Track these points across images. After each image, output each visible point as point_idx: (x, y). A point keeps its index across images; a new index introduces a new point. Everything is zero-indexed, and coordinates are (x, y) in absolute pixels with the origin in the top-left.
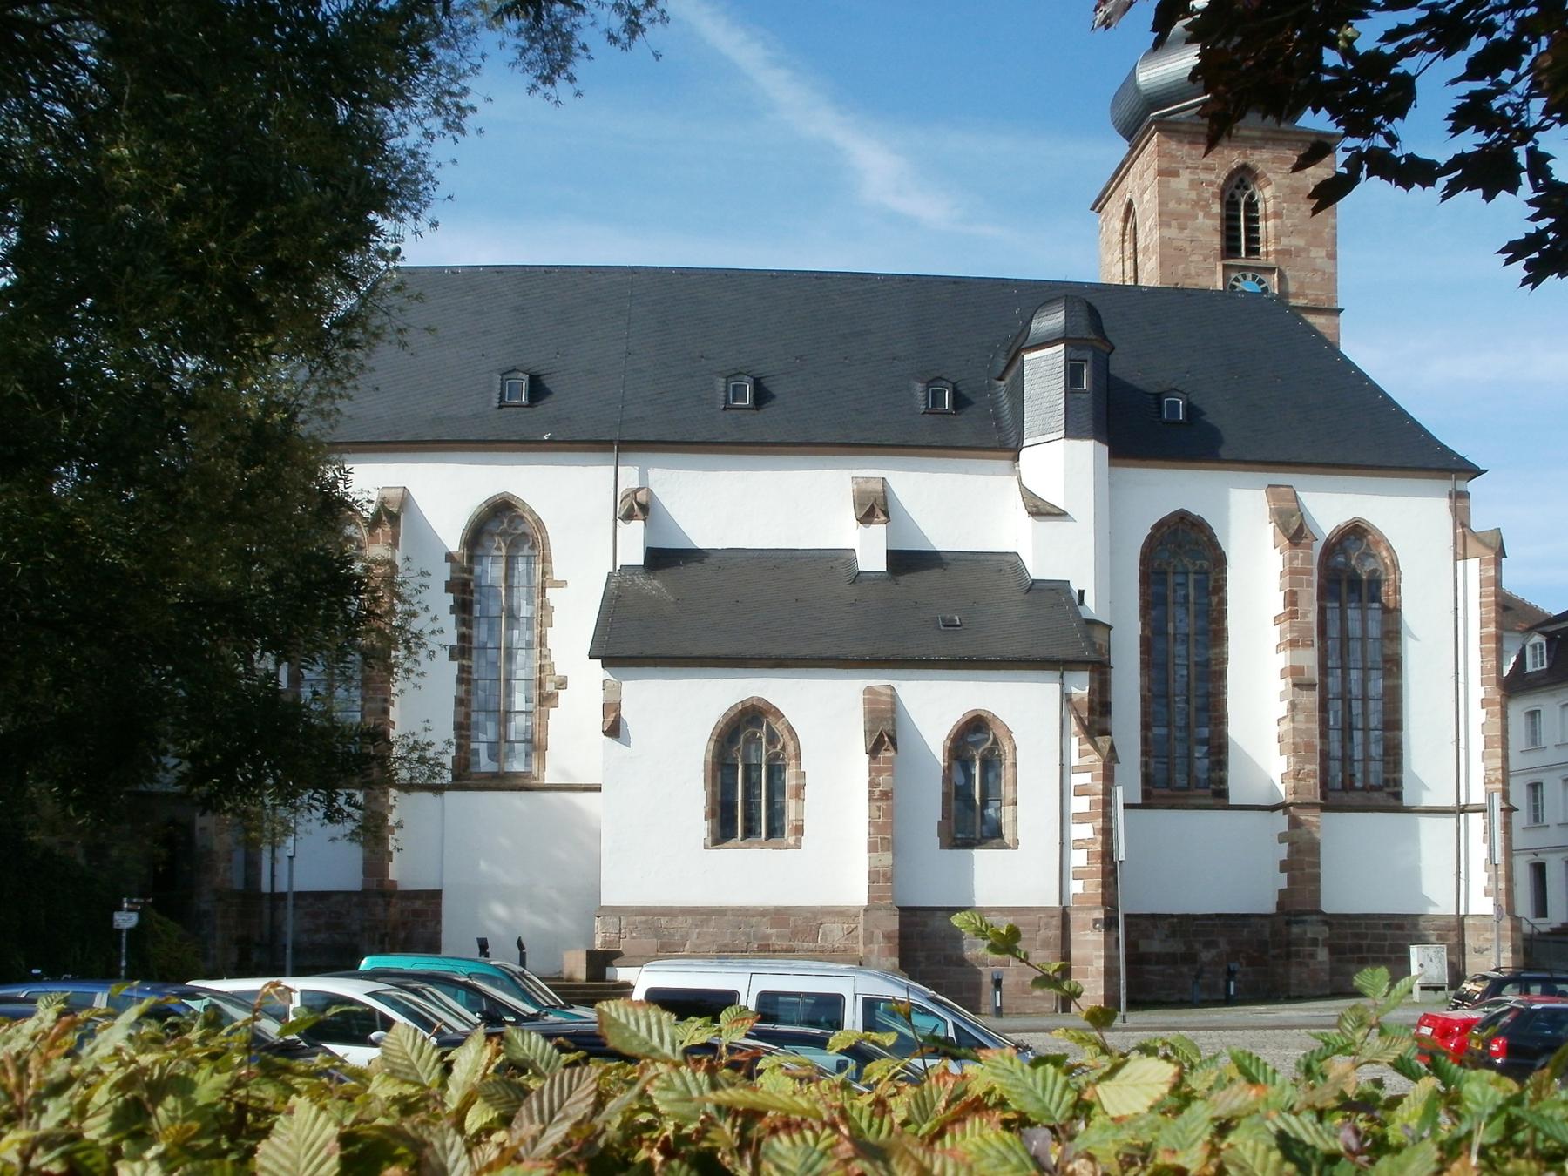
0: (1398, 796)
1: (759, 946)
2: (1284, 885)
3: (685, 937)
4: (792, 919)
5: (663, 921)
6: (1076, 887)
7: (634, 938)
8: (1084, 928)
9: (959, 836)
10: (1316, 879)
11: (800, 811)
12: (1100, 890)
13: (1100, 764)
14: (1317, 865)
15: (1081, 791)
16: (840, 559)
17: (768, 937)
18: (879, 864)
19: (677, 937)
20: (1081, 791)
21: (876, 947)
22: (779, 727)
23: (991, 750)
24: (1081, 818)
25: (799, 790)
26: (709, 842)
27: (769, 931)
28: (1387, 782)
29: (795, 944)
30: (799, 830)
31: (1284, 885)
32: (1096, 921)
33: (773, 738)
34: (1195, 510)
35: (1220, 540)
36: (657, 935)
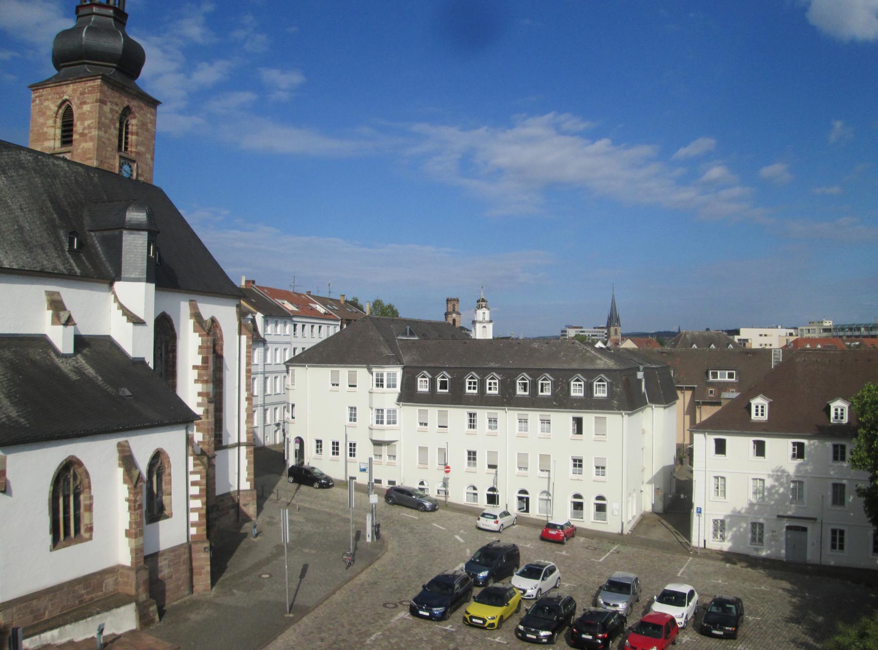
1: (80, 601)
5: (35, 602)
6: (193, 531)
7: (20, 618)
8: (199, 551)
11: (91, 518)
12: (205, 532)
13: (204, 471)
15: (194, 484)
16: (42, 341)
19: (42, 610)
20: (194, 484)
22: (80, 470)
23: (159, 467)
24: (195, 497)
30: (90, 529)
33: (75, 477)
35: (175, 327)
36: (32, 612)
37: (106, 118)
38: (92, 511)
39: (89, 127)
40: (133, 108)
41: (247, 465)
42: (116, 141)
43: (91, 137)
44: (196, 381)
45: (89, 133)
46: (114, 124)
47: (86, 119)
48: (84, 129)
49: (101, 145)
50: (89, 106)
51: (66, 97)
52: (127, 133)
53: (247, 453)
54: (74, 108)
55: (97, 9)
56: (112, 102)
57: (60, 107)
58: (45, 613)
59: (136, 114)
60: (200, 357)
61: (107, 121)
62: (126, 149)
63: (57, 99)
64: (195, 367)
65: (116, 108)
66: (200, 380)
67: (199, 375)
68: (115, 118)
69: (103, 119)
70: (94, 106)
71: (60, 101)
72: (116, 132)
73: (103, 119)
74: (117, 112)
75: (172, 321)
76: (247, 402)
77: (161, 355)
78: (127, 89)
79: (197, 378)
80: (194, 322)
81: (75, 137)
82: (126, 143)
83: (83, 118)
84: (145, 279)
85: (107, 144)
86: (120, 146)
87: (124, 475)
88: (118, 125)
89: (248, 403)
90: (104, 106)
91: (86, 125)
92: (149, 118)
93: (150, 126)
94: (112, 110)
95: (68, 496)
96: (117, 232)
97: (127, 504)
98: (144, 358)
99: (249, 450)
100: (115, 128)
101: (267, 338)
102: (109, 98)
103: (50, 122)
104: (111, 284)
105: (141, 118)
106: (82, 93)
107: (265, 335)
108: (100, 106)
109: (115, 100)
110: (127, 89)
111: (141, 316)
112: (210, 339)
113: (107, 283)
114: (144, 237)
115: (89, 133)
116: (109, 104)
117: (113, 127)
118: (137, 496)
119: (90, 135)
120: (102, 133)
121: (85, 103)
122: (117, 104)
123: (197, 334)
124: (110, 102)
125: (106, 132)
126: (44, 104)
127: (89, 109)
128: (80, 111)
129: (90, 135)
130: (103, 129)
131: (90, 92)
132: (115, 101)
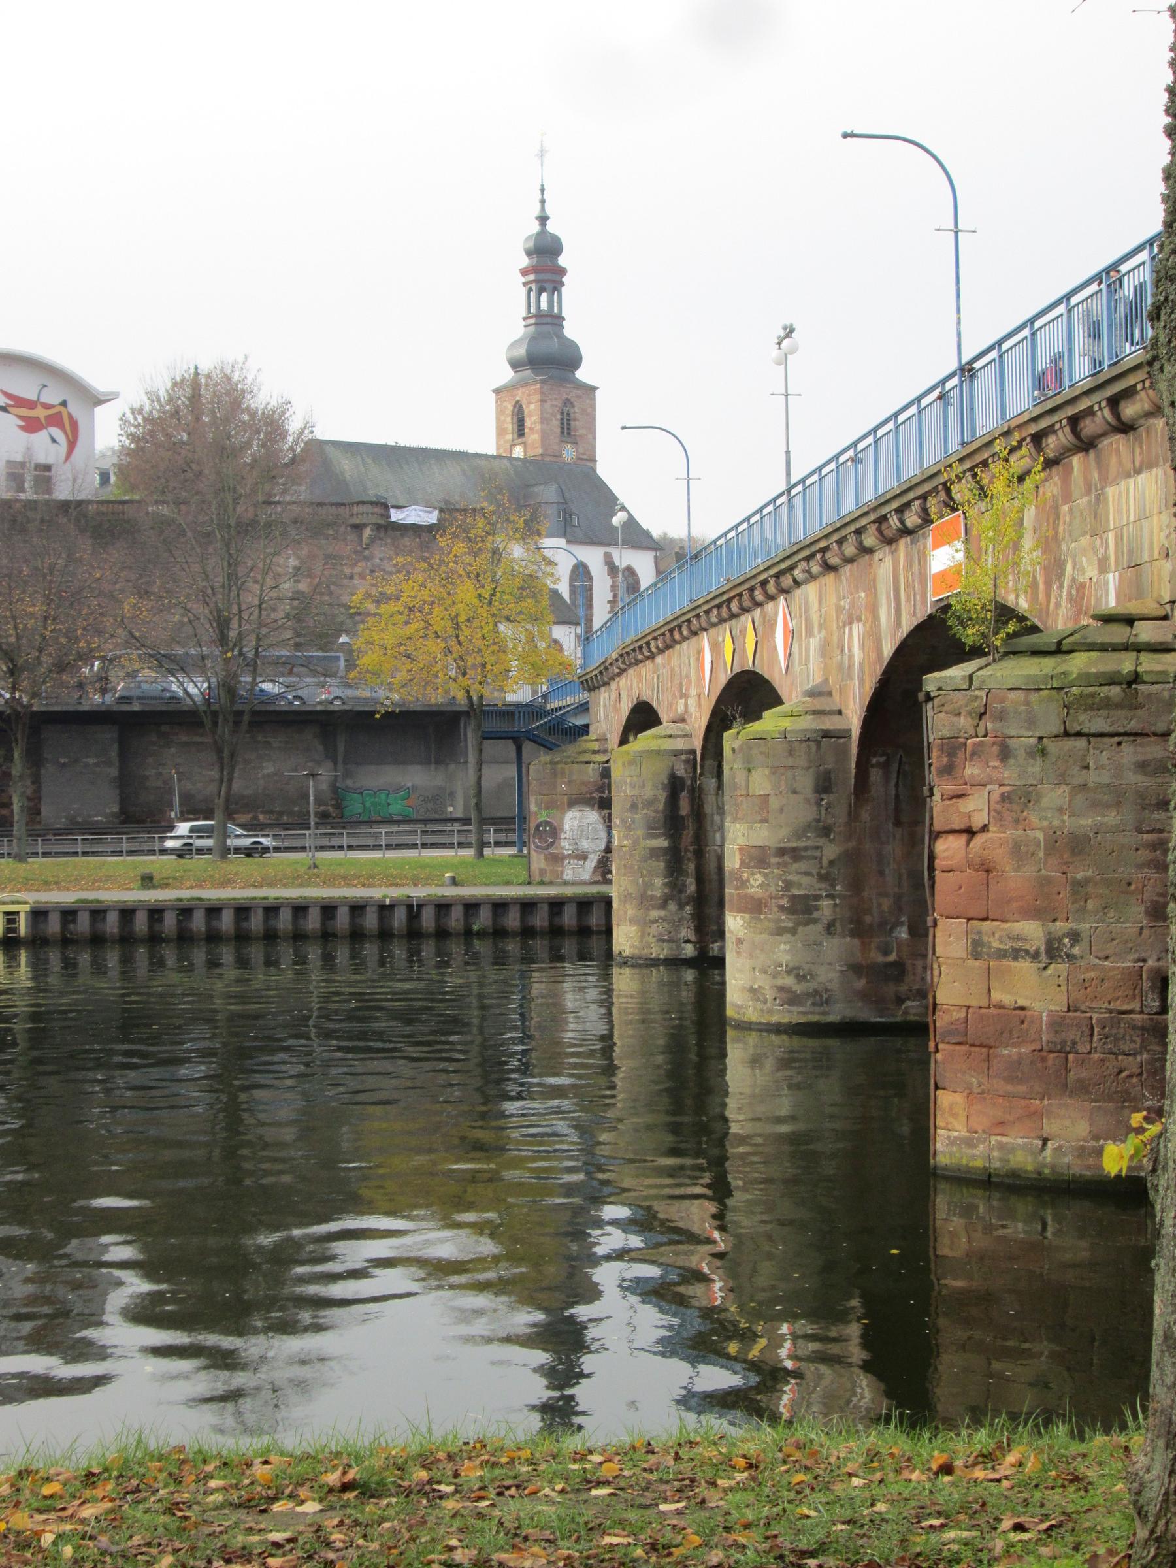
39: (535, 423)
42: (558, 430)
49: (544, 436)
57: (515, 406)
62: (569, 433)
64: (609, 602)
65: (555, 403)
67: (612, 608)
72: (558, 423)
81: (526, 430)
83: (530, 416)
86: (562, 433)
88: (559, 417)
93: (589, 410)
94: (553, 406)
103: (509, 420)
121: (530, 403)
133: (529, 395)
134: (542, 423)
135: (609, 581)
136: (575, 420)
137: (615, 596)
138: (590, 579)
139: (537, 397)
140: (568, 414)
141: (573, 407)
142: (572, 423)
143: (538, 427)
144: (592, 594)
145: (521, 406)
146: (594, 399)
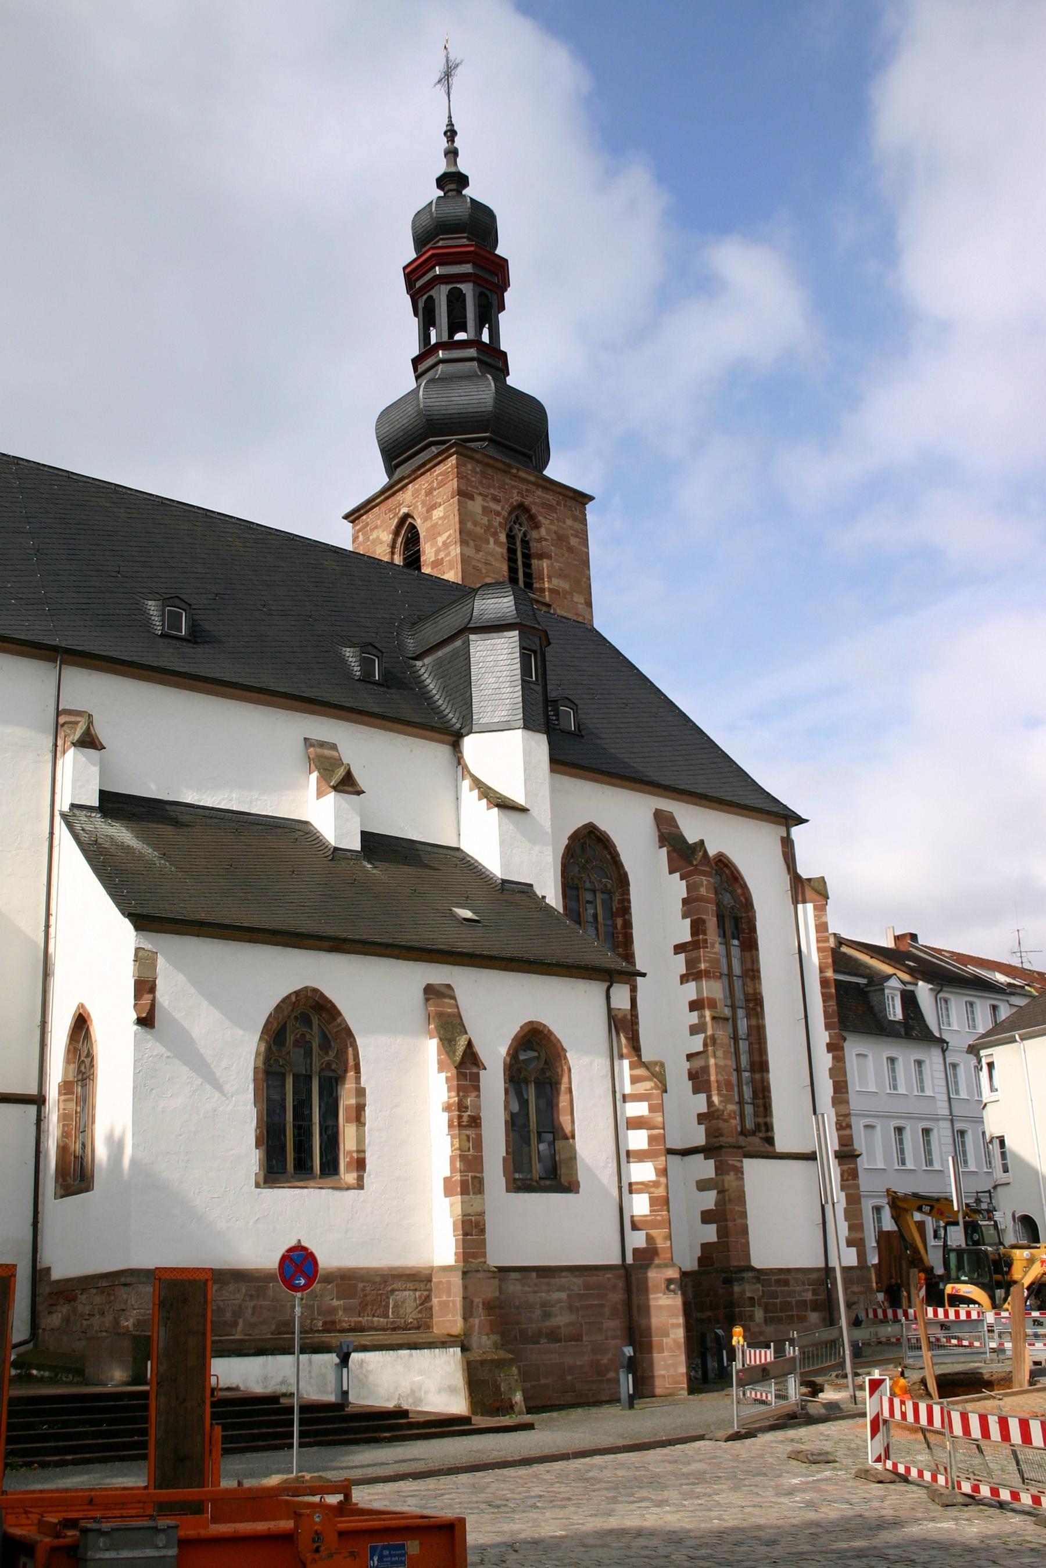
0: (770, 1141)
2: (713, 1238)
3: (238, 1313)
4: (360, 1285)
9: (517, 1176)
10: (744, 1230)
11: (360, 1139)
14: (744, 1215)
17: (333, 1310)
18: (471, 1210)
19: (229, 1314)
21: (477, 1321)
25: (359, 1114)
26: (261, 1180)
27: (335, 1303)
28: (758, 1125)
29: (365, 1320)
30: (360, 1165)
31: (713, 1238)
32: (670, 1281)
34: (602, 826)
37: (475, 524)
38: (365, 1124)
39: (446, 545)
40: (533, 506)
41: (845, 1206)
43: (450, 561)
44: (684, 979)
45: (446, 556)
46: (495, 534)
47: (440, 534)
48: (437, 553)
50: (441, 508)
51: (404, 510)
52: (527, 556)
53: (842, 1175)
54: (418, 523)
55: (446, 352)
56: (486, 496)
57: (396, 533)
58: (235, 1324)
59: (540, 518)
60: (688, 921)
61: (479, 530)
63: (390, 519)
64: (679, 949)
66: (692, 974)
67: (690, 964)
68: (496, 524)
69: (470, 525)
70: (451, 505)
71: (396, 520)
73: (470, 525)
74: (498, 514)
75: (614, 847)
76: (830, 1055)
77: (595, 916)
78: (514, 471)
79: (684, 972)
80: (668, 853)
82: (528, 575)
83: (433, 537)
84: (521, 723)
85: (484, 571)
87: (439, 1054)
88: (503, 538)
89: (834, 1058)
90: (470, 503)
91: (440, 544)
92: (571, 528)
93: (574, 541)
94: (486, 510)
95: (309, 1078)
96: (458, 643)
97: (445, 1116)
98: (531, 886)
99: (846, 1167)
100: (497, 542)
101: (945, 1037)
102: (477, 488)
104: (456, 746)
105: (554, 528)
106: (429, 493)
107: (940, 1029)
108: (459, 501)
109: (492, 491)
110: (514, 471)
111: (520, 799)
112: (705, 882)
113: (447, 744)
114: (511, 640)
115: (446, 556)
116: (479, 500)
117: (492, 540)
118: (466, 1097)
119: (448, 558)
120: (470, 552)
122: (496, 500)
123: (677, 875)
124: (480, 494)
125: (478, 549)
126: (371, 538)
127: (442, 514)
128: (428, 524)
129: (448, 558)
130: (472, 543)
131: (441, 485)
132: (492, 494)
133: (429, 493)
134: (463, 542)
135: (677, 888)
136: (541, 556)
137: (697, 928)
138: (623, 881)
139: (454, 484)
140: (525, 543)
141: (537, 526)
142: (535, 562)
143: (456, 551)
144: (628, 925)
145: (413, 528)
146: (584, 521)
